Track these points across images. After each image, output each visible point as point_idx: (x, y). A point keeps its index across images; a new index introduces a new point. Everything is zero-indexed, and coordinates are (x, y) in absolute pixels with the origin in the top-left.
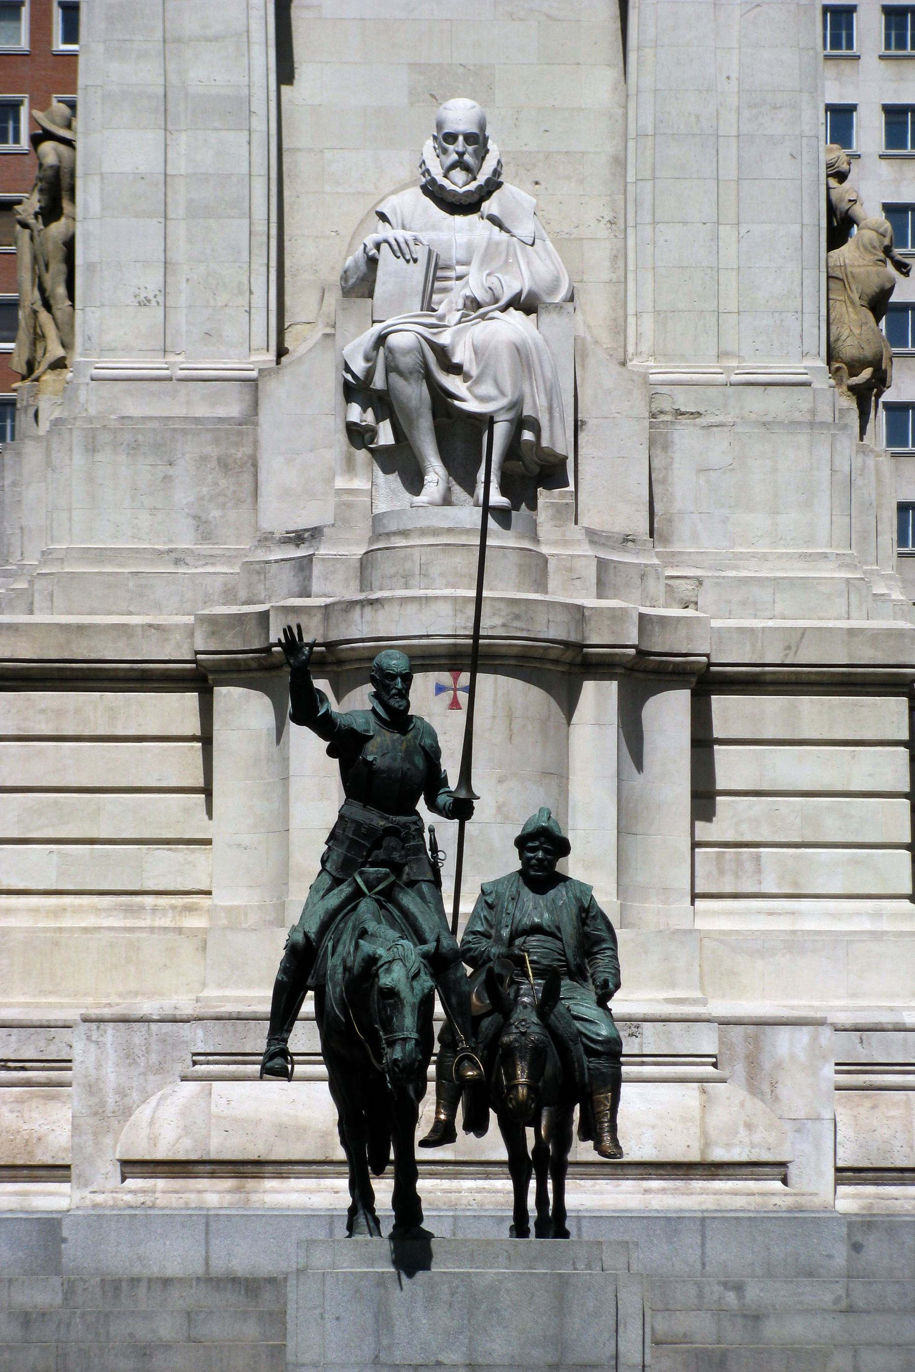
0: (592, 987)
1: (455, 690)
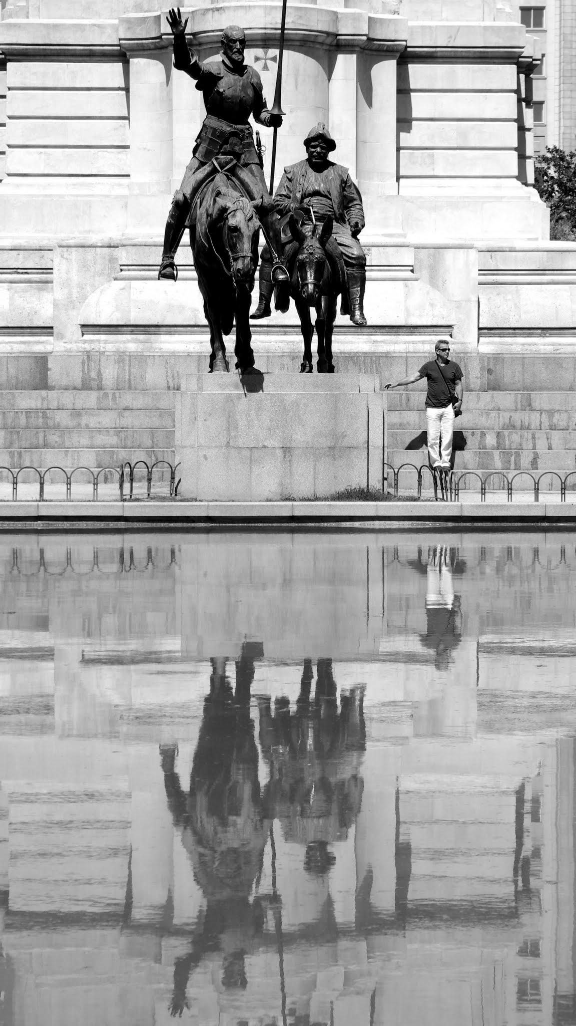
0: (348, 227)
1: (266, 59)
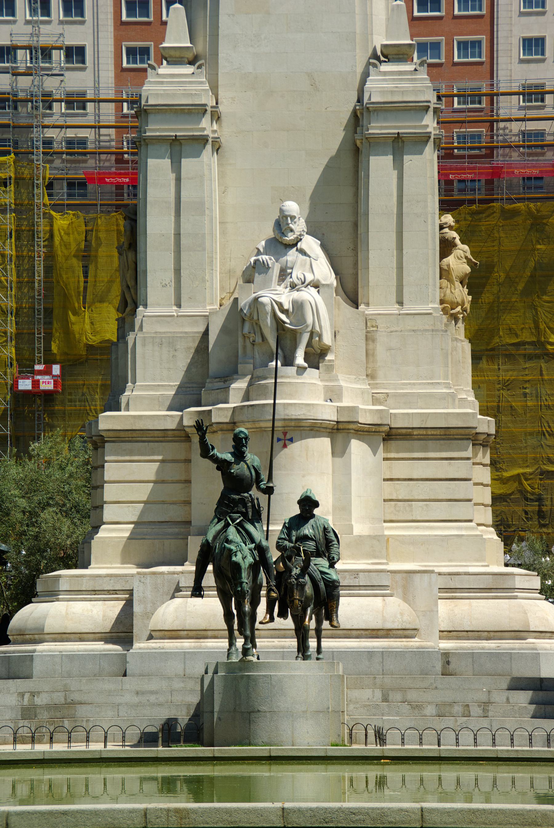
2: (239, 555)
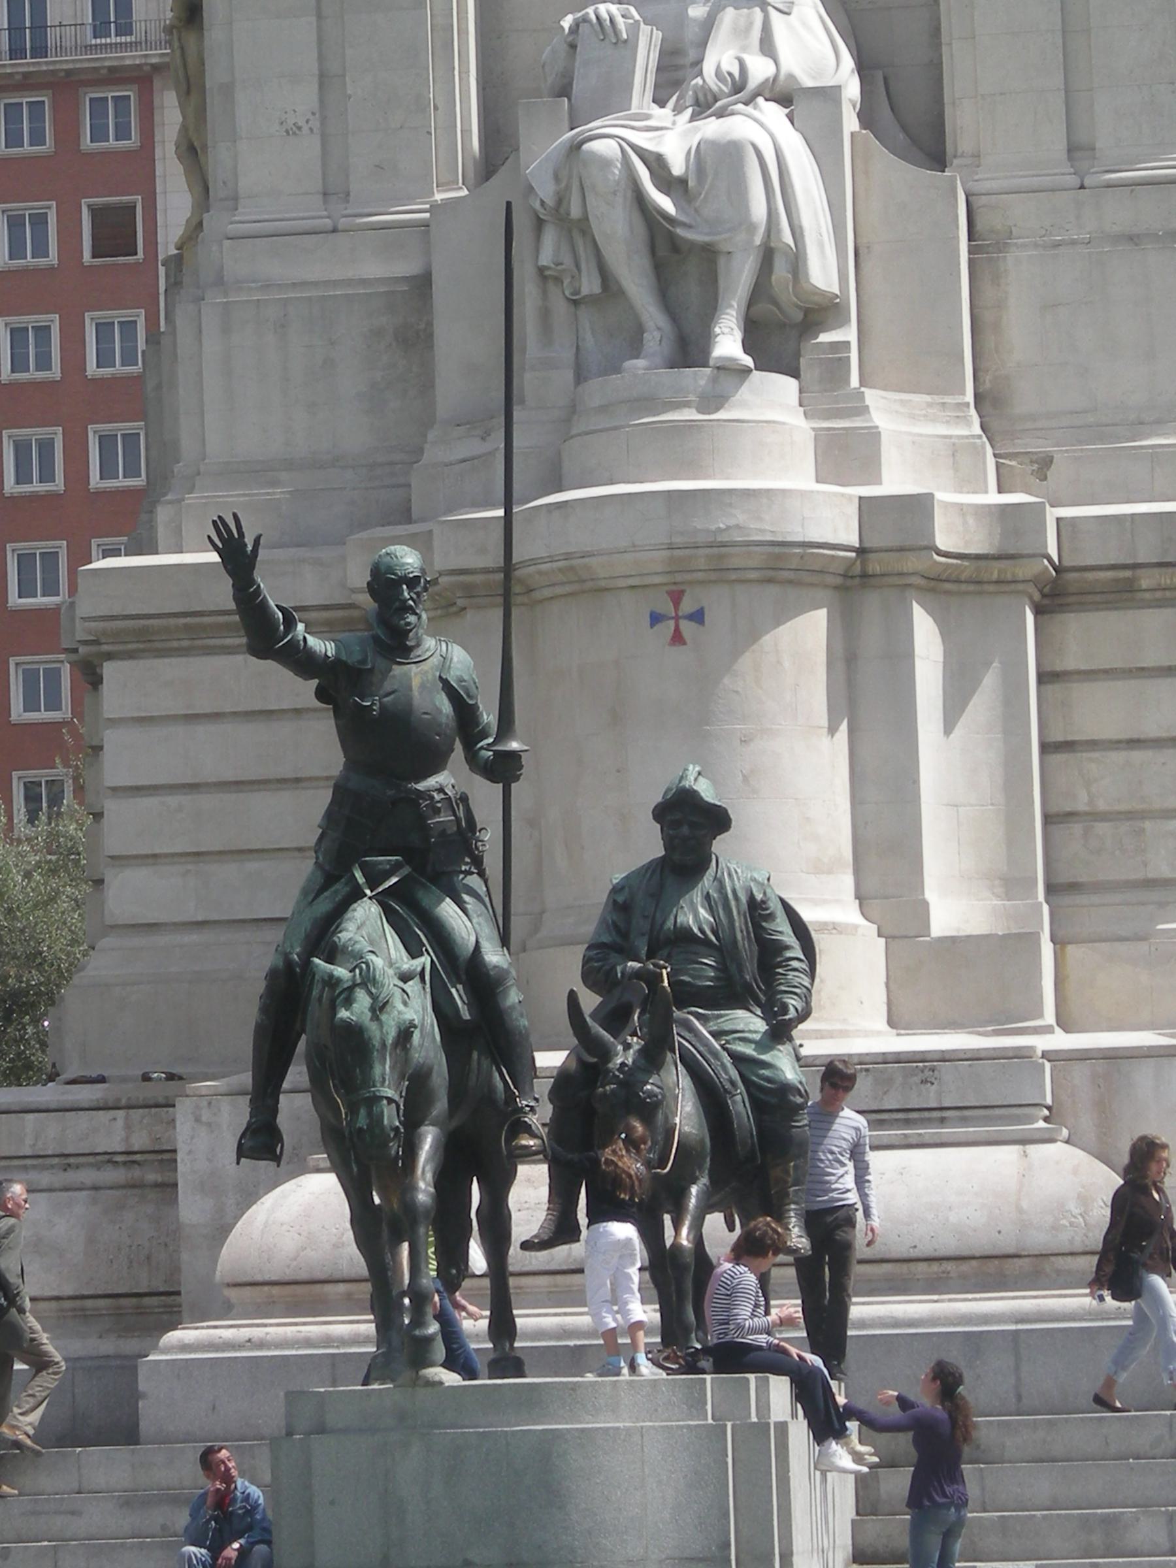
1: (677, 618)
2: (362, 1001)
